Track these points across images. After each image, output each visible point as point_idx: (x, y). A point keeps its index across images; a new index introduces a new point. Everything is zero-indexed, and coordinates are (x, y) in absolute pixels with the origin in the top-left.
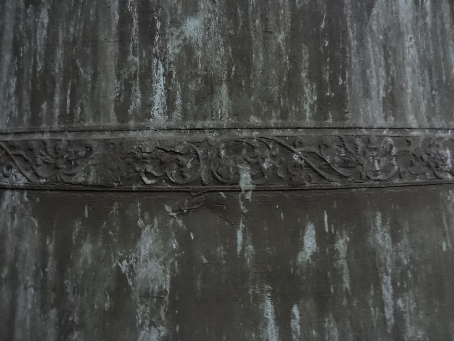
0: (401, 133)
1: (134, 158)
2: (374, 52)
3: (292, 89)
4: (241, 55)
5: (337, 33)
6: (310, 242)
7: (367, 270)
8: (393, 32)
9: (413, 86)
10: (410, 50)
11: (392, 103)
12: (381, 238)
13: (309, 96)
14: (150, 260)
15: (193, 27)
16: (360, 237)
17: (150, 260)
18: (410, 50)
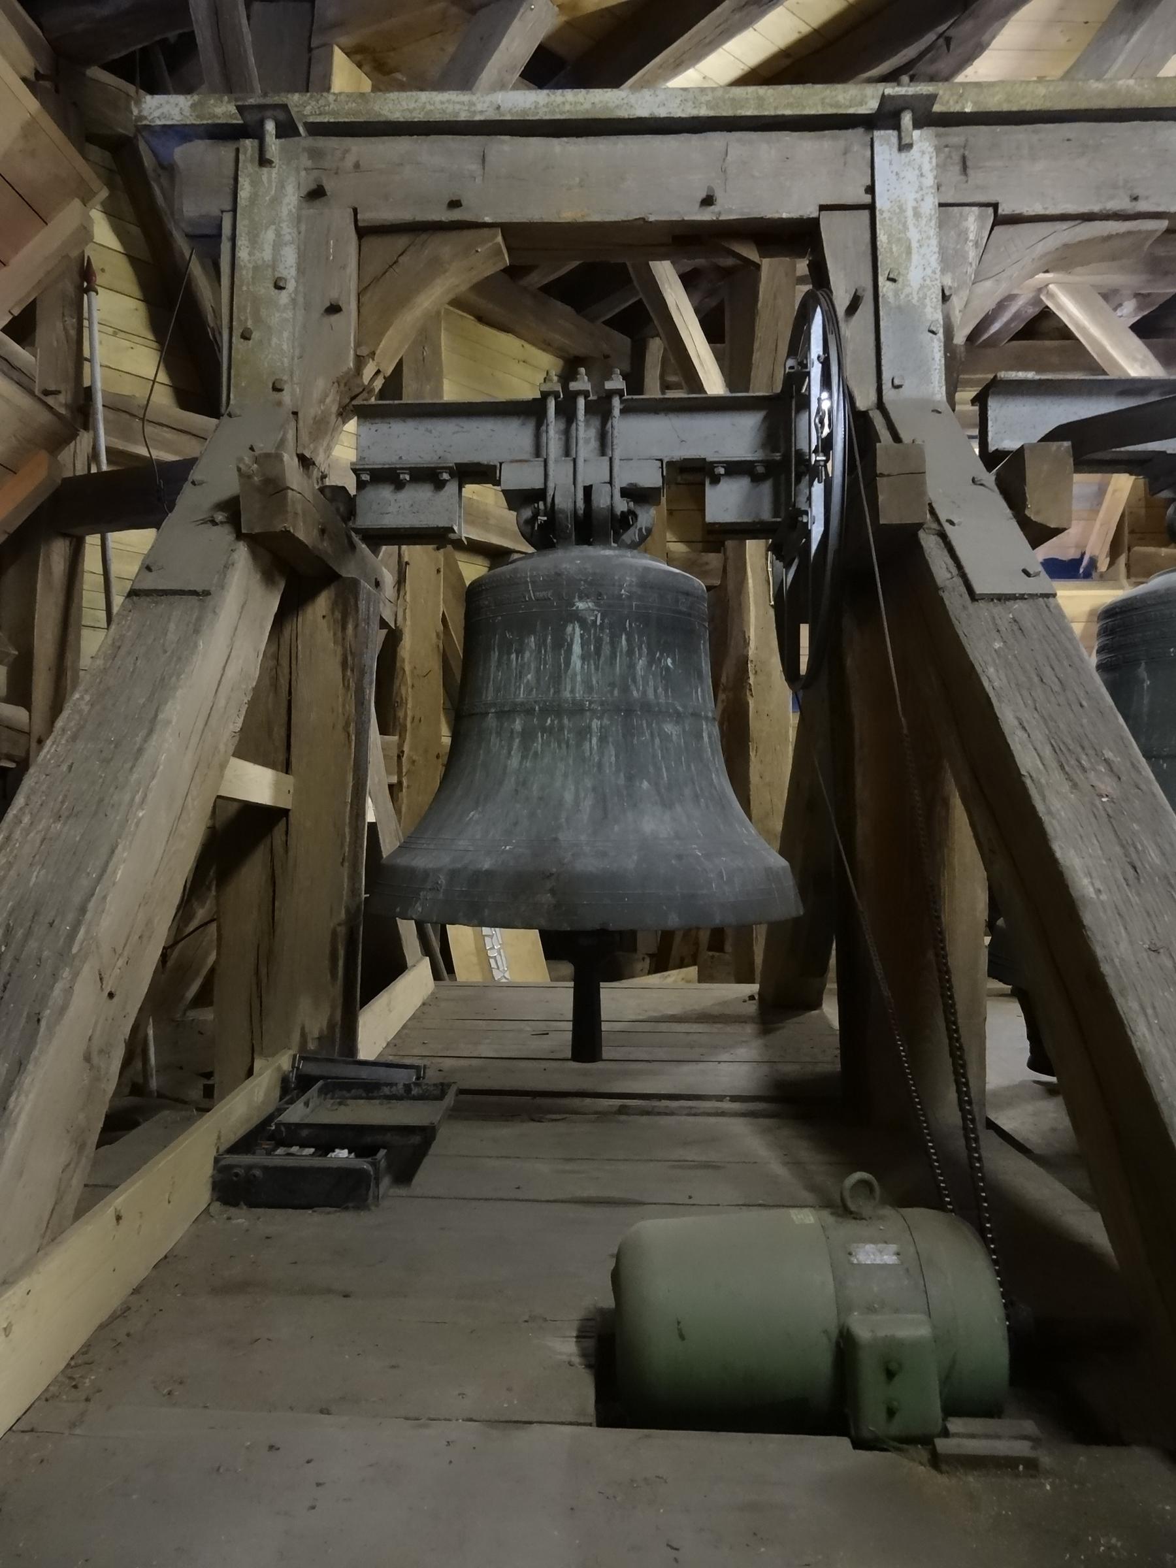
0: (574, 699)
1: (516, 704)
2: (568, 680)
3: (549, 688)
4: (538, 680)
5: (560, 677)
6: (549, 721)
7: (561, 728)
8: (575, 675)
9: (579, 688)
10: (579, 678)
11: (572, 691)
12: (566, 721)
13: (552, 691)
14: (518, 725)
15: (529, 676)
16: (560, 721)
17: (518, 725)
18: (579, 678)
